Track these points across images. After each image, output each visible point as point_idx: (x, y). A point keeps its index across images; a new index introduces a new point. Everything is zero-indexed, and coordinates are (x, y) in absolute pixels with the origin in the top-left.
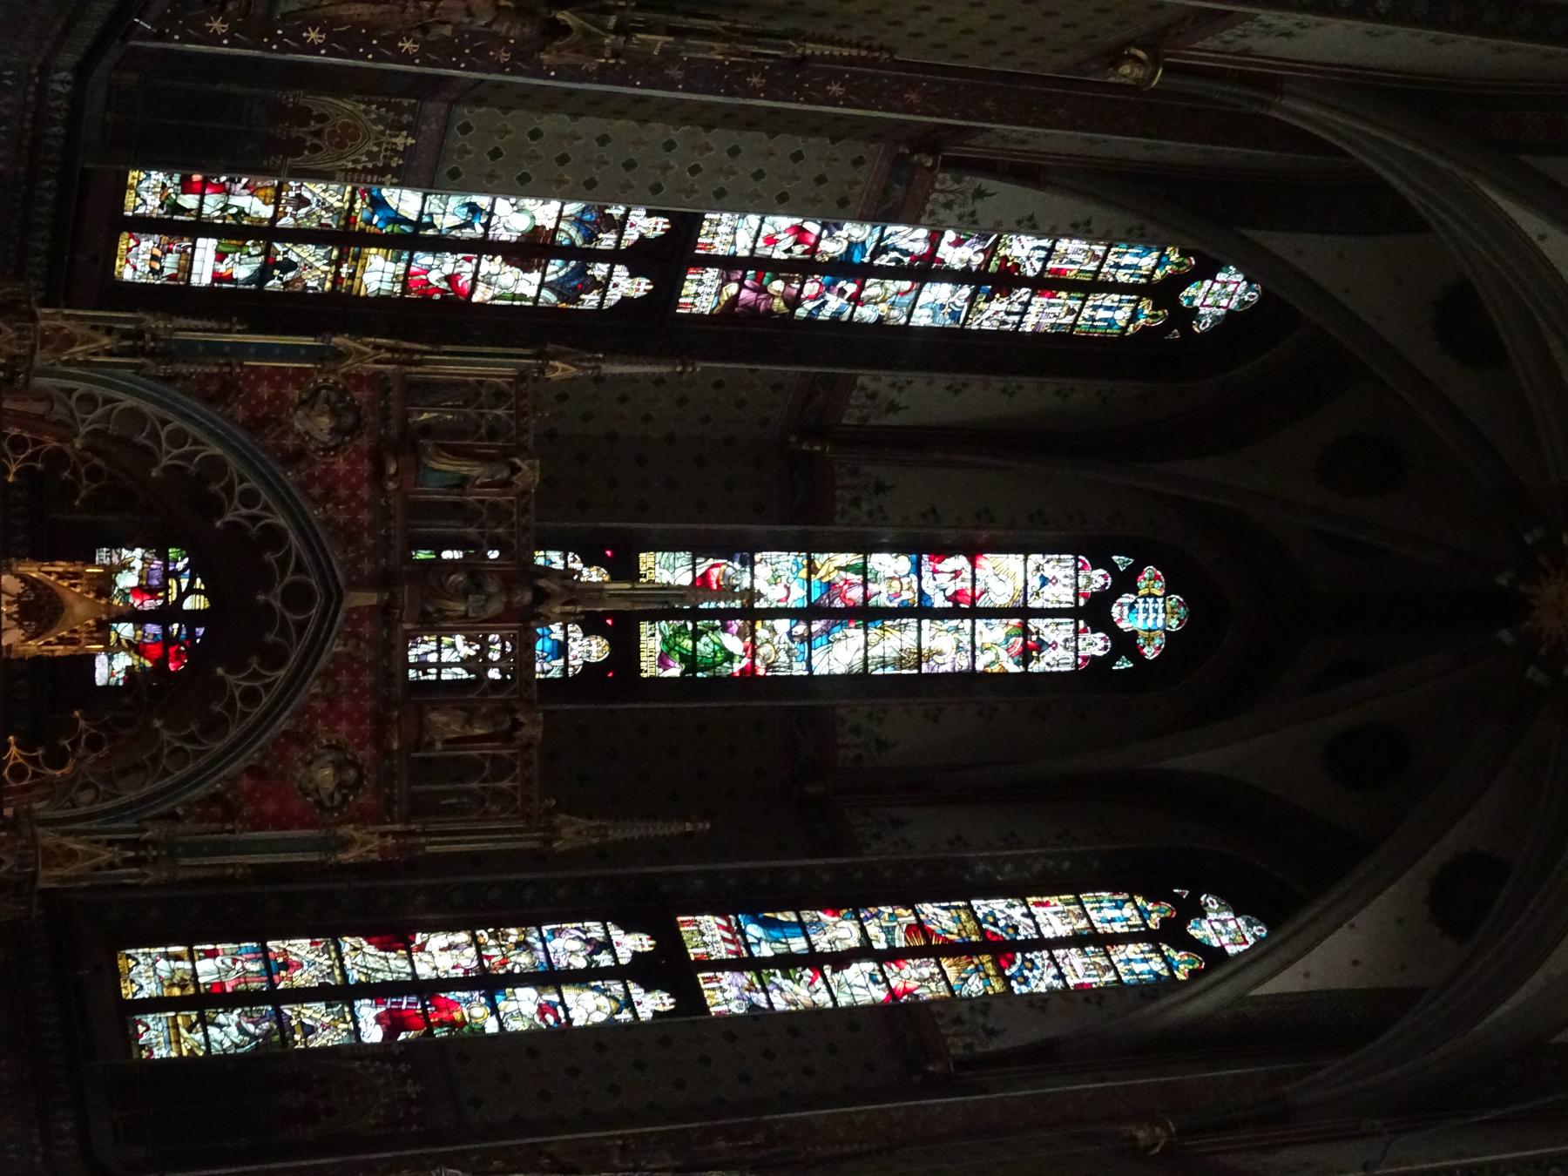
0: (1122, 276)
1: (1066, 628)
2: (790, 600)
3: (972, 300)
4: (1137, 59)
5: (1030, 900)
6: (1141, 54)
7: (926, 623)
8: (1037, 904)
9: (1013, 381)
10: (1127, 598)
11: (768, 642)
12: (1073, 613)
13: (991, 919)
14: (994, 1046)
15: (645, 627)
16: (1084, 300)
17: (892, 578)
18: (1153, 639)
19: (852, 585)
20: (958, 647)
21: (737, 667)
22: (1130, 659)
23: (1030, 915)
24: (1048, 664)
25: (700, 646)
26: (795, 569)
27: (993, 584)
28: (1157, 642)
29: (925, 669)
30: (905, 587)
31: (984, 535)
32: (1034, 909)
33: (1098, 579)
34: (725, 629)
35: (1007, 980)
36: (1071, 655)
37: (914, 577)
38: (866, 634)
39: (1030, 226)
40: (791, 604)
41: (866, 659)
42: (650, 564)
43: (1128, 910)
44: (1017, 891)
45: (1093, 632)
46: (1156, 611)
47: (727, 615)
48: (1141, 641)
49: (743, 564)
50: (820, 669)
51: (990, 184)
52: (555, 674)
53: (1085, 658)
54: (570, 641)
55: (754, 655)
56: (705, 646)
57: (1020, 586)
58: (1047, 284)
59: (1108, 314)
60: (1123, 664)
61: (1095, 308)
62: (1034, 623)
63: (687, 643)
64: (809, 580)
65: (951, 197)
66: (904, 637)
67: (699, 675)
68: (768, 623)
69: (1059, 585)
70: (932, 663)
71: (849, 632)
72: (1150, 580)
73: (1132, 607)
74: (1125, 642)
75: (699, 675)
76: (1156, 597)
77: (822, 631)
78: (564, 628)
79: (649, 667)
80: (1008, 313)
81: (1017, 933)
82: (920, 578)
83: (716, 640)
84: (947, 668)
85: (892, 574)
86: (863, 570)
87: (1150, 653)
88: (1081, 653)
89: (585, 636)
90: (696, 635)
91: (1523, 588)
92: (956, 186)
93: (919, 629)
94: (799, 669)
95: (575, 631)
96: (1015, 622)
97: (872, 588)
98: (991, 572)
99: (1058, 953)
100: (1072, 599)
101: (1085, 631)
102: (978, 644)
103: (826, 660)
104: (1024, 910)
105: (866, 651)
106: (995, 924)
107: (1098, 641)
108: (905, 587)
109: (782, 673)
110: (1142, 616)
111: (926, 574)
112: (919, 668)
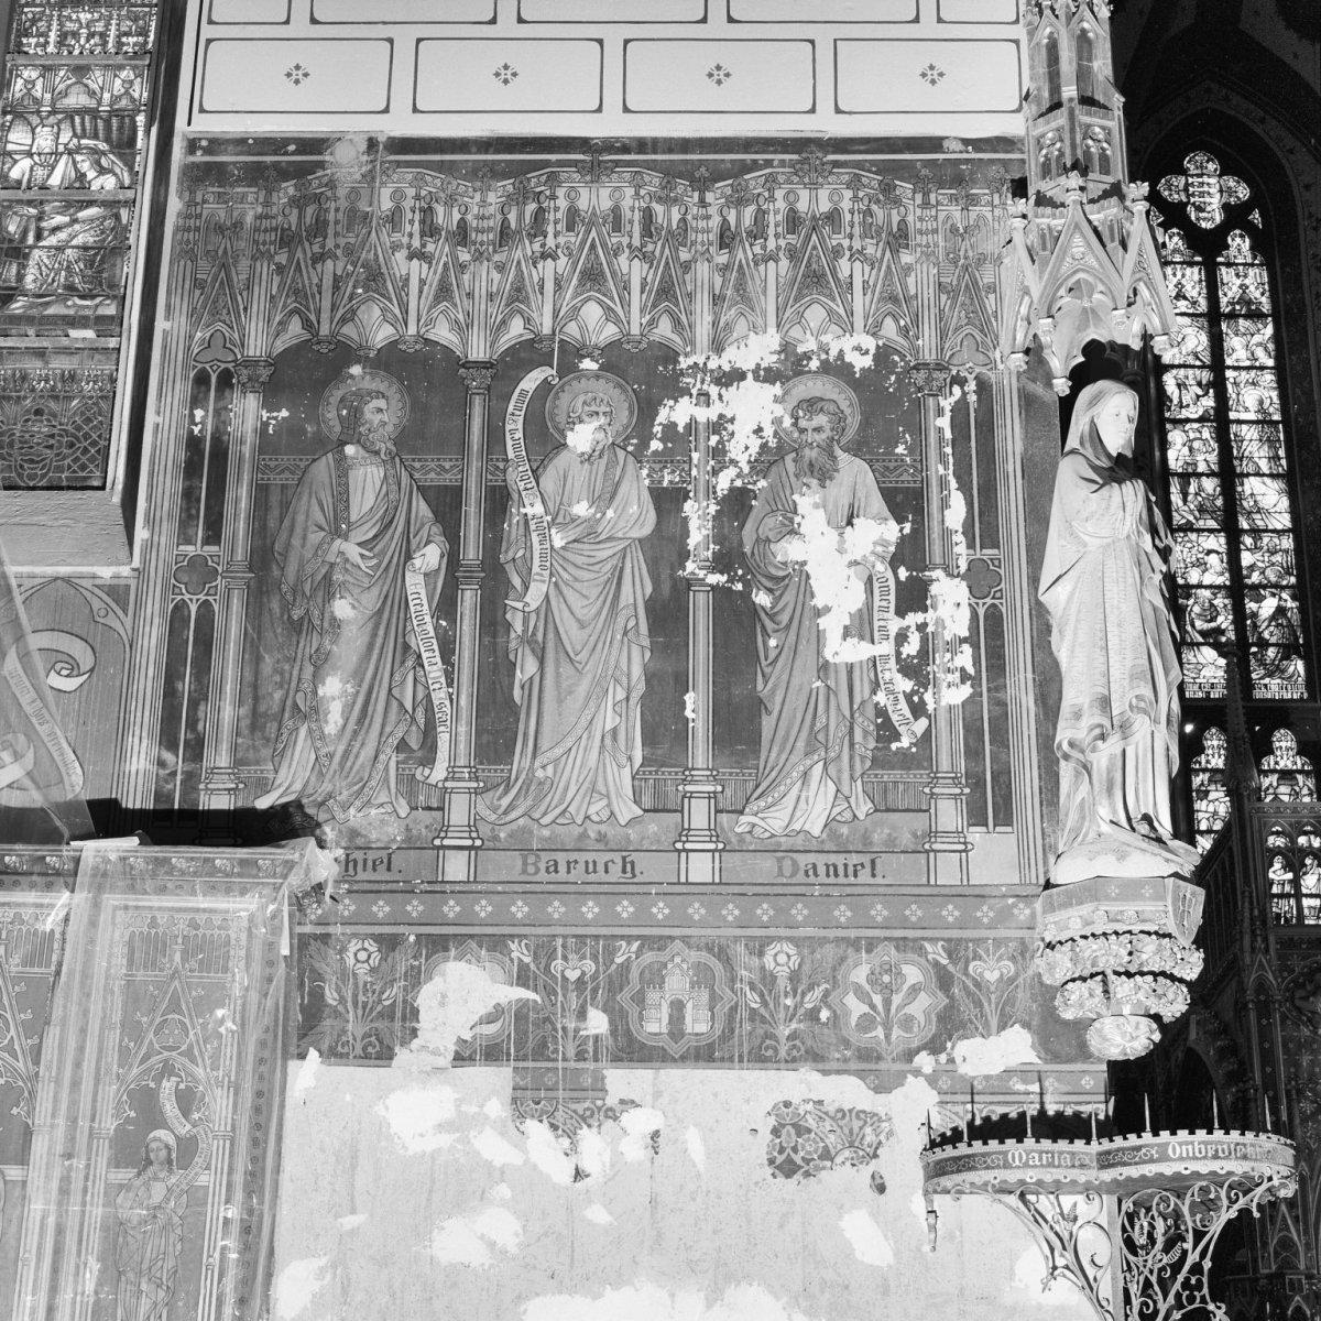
1: (1226, 274)
2: (1221, 550)
7: (1232, 415)
11: (1263, 573)
15: (1258, 694)
17: (1191, 449)
18: (1229, 188)
19: (1200, 489)
20: (1253, 384)
21: (1290, 604)
24: (1263, 294)
25: (1273, 640)
26: (1189, 545)
27: (1191, 344)
28: (1232, 184)
29: (1277, 417)
30: (1198, 435)
34: (1255, 615)
36: (1251, 272)
37: (1188, 427)
38: (1248, 475)
40: (1223, 549)
41: (1271, 476)
42: (1196, 687)
45: (1227, 247)
46: (1202, 184)
47: (1240, 615)
49: (1188, 597)
50: (1284, 521)
52: (1311, 783)
53: (1255, 258)
54: (1209, 766)
55: (1276, 586)
56: (1270, 634)
57: (1187, 320)
60: (1256, 217)
63: (1271, 652)
64: (1199, 531)
66: (1248, 437)
67: (1301, 641)
68: (1245, 572)
69: (1184, 281)
70: (1271, 410)
71: (1248, 492)
73: (1199, 209)
74: (1235, 216)
75: (1301, 641)
76: (1187, 185)
77: (1248, 519)
78: (1266, 773)
79: (1296, 692)
82: (1188, 420)
83: (1266, 624)
84: (1274, 394)
85: (1186, 448)
86: (1185, 477)
87: (1243, 192)
88: (1249, 260)
89: (1272, 753)
90: (1263, 644)
93: (1240, 422)
94: (1287, 543)
95: (1268, 762)
97: (1202, 468)
98: (1176, 350)
100: (1196, 269)
102: (1248, 363)
103: (1276, 515)
105: (1264, 475)
107: (1235, 244)
108: (1198, 435)
109: (1291, 559)
110: (1208, 200)
111: (1185, 414)
112: (1277, 422)
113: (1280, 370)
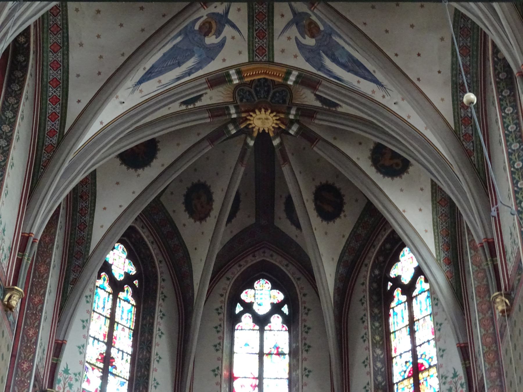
0: (109, 305)
3: (115, 375)
4: (10, 298)
5: (394, 355)
6: (7, 296)
8: (395, 352)
9: (153, 357)
10: (255, 307)
12: (262, 331)
13: (403, 373)
14: (461, 372)
16: (118, 323)
22: (283, 306)
23: (401, 355)
31: (225, 373)
32: (398, 353)
33: (247, 320)
35: (430, 367)
39: (82, 348)
43: (398, 309)
44: (389, 360)
48: (275, 302)
51: (62, 367)
53: (283, 327)
58: (110, 342)
59: (125, 312)
60: (285, 309)
61: (122, 319)
62: (266, 351)
65: (67, 385)
72: (247, 296)
73: (260, 305)
74: (276, 308)
80: (122, 359)
81: (409, 362)
91: (255, 134)
92: (62, 382)
96: (265, 358)
99: (418, 343)
101: (270, 327)
104: (399, 357)
106: (405, 372)
113: (290, 380)
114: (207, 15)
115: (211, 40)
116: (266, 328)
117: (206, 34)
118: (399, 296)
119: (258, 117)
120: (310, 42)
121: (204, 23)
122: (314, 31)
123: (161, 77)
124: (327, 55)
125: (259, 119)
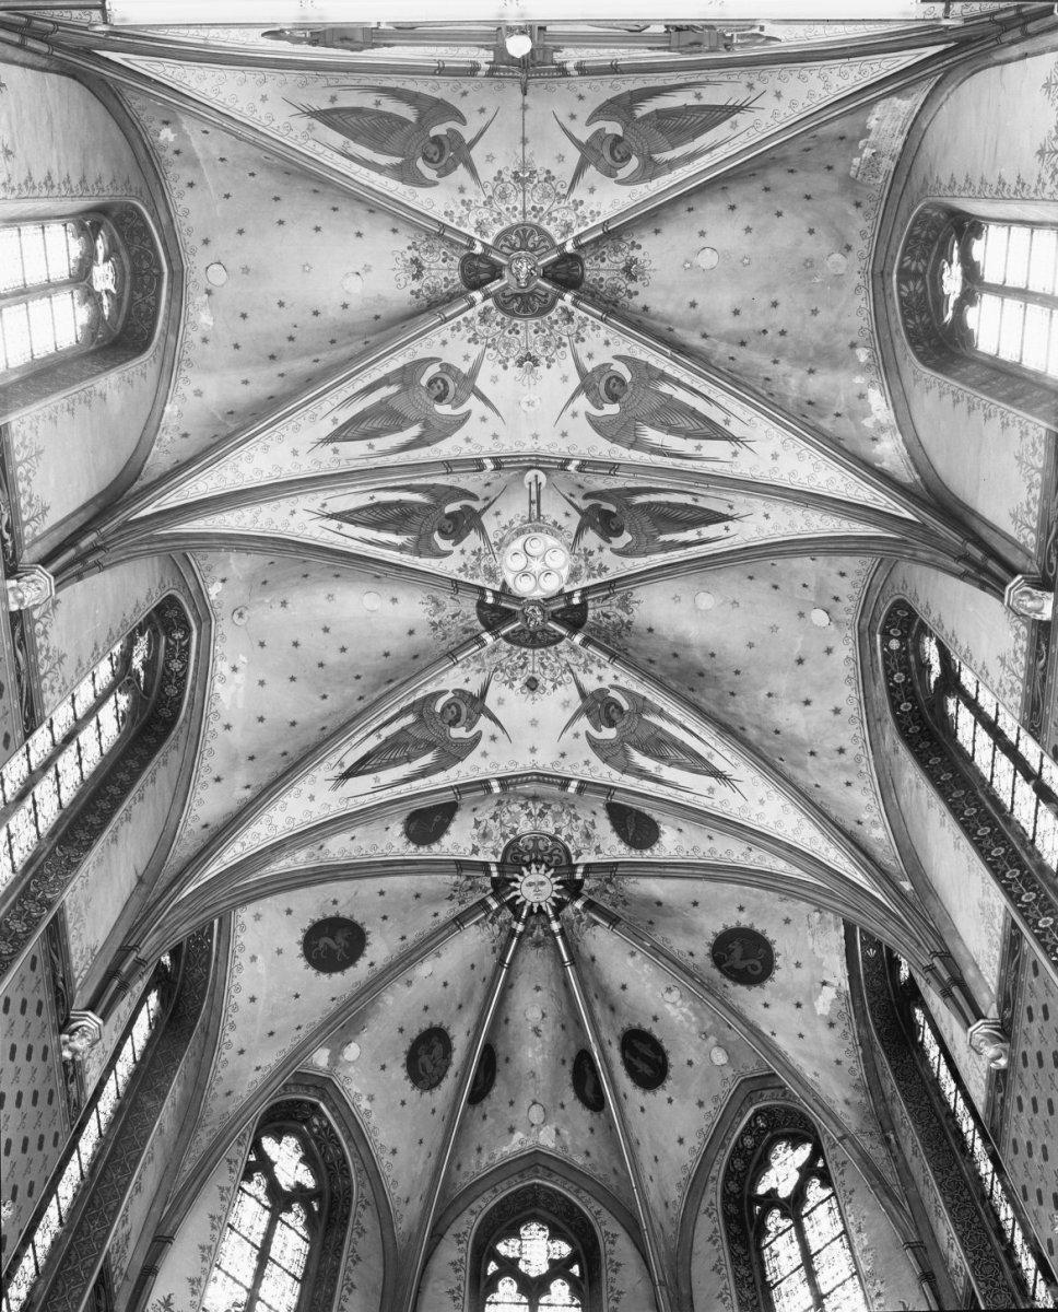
10: (522, 1266)
33: (507, 1288)
59: (289, 1248)
60: (576, 1270)
74: (558, 1268)
114: (454, 691)
115: (458, 732)
116: (543, 1300)
117: (453, 723)
118: (775, 1220)
119: (531, 879)
120: (609, 733)
121: (448, 706)
122: (615, 716)
123: (380, 774)
124: (636, 748)
125: (530, 884)
